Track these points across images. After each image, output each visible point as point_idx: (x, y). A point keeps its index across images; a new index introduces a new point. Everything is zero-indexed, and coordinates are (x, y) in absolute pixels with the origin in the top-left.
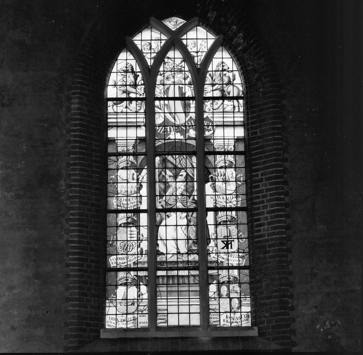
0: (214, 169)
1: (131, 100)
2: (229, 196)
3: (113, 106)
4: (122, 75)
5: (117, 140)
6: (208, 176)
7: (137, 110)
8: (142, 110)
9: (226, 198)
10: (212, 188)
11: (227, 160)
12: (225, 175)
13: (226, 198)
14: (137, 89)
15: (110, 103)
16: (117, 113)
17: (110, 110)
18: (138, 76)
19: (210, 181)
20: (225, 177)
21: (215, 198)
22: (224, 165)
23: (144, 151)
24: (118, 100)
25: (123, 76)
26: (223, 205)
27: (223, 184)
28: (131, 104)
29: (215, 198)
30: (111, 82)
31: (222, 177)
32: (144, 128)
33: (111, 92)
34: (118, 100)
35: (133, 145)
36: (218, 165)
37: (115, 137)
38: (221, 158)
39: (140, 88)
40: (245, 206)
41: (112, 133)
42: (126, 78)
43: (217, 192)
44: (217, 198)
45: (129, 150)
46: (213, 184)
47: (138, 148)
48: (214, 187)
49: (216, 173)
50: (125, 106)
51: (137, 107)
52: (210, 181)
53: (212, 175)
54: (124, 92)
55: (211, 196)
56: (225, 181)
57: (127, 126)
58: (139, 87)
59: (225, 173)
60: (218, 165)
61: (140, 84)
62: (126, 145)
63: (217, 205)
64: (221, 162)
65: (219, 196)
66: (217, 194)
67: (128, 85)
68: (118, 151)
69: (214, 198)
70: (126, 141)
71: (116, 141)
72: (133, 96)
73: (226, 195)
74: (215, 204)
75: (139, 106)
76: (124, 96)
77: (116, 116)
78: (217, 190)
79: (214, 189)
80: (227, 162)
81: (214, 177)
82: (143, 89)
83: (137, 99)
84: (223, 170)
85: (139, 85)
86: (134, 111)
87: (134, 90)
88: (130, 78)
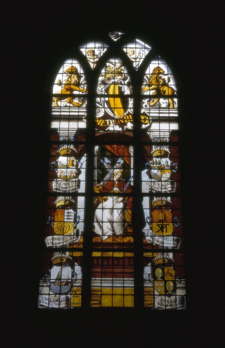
1: (73, 96)
3: (57, 101)
4: (67, 76)
5: (59, 130)
7: (79, 105)
8: (84, 106)
14: (80, 88)
15: (55, 99)
16: (61, 107)
17: (54, 104)
18: (82, 77)
23: (84, 140)
24: (61, 97)
25: (68, 77)
28: (75, 100)
30: (56, 81)
32: (85, 120)
33: (57, 89)
34: (61, 97)
35: (74, 135)
37: (57, 128)
39: (83, 87)
41: (55, 125)
42: (71, 78)
45: (70, 140)
47: (79, 138)
50: (68, 101)
51: (80, 102)
54: (67, 90)
57: (69, 119)
58: (82, 86)
61: (83, 83)
62: (67, 135)
67: (72, 84)
68: (60, 140)
70: (67, 131)
71: (58, 131)
72: (75, 93)
75: (81, 102)
76: (68, 93)
77: (59, 110)
82: (85, 87)
83: (79, 96)
85: (82, 84)
86: (76, 106)
87: (78, 89)
88: (74, 79)
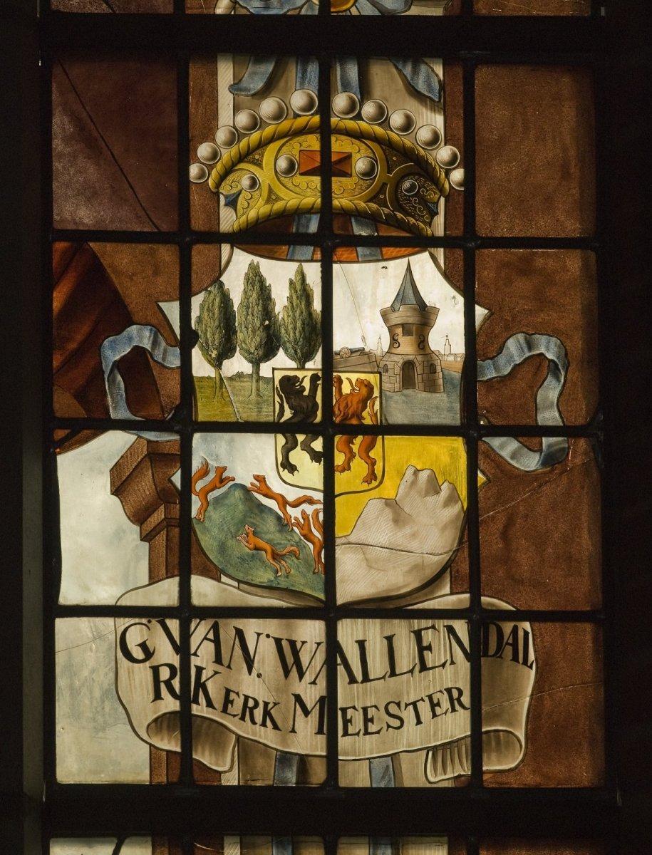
0: (167, 255)
2: (373, 631)
6: (92, 345)
9: (333, 648)
10: (139, 517)
11: (359, 136)
12: (318, 332)
13: (333, 648)
19: (120, 412)
20: (316, 363)
21: (183, 649)
22: (303, 193)
26: (284, 758)
27: (299, 457)
29: (183, 649)
31: (282, 362)
36: (232, 203)
38: (268, 107)
40: (580, 770)
43: (213, 573)
44: (203, 655)
46: (155, 456)
48: (164, 495)
49: (196, 302)
52: (120, 412)
53: (140, 336)
55: (123, 622)
56: (321, 419)
59: (317, 305)
60: (232, 203)
63: (204, 756)
64: (275, 159)
65: (228, 628)
66: (205, 591)
69: (166, 654)
73: (330, 611)
74: (171, 744)
78: (208, 540)
79: (167, 523)
80: (360, 165)
81: (174, 361)
84: (279, 275)
